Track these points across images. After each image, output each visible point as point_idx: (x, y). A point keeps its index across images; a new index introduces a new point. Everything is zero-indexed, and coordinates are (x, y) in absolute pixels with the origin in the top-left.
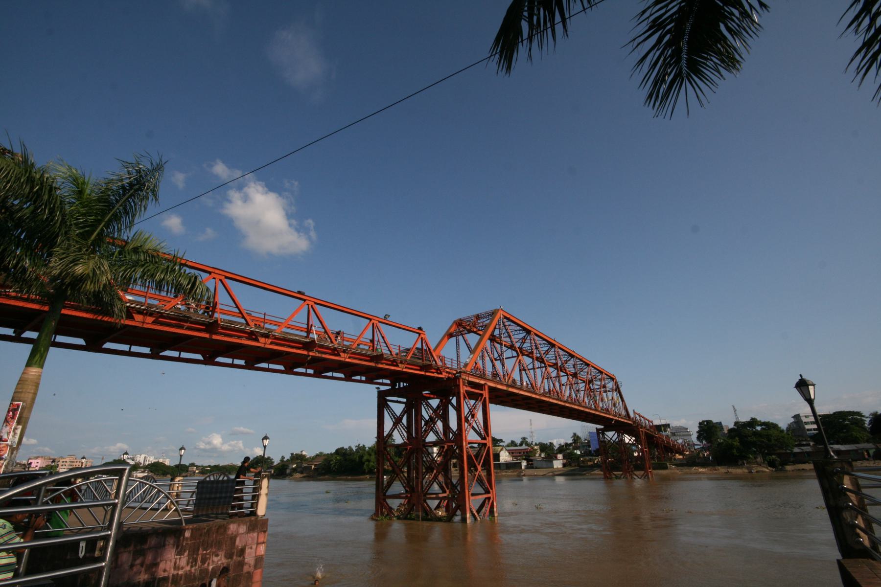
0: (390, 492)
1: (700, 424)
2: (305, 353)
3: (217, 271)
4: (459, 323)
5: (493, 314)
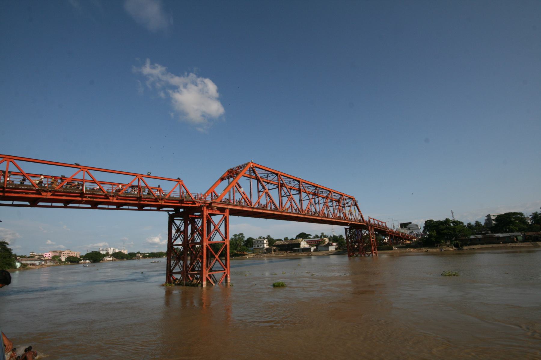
0: (174, 271)
1: (426, 222)
3: (7, 157)
5: (247, 164)
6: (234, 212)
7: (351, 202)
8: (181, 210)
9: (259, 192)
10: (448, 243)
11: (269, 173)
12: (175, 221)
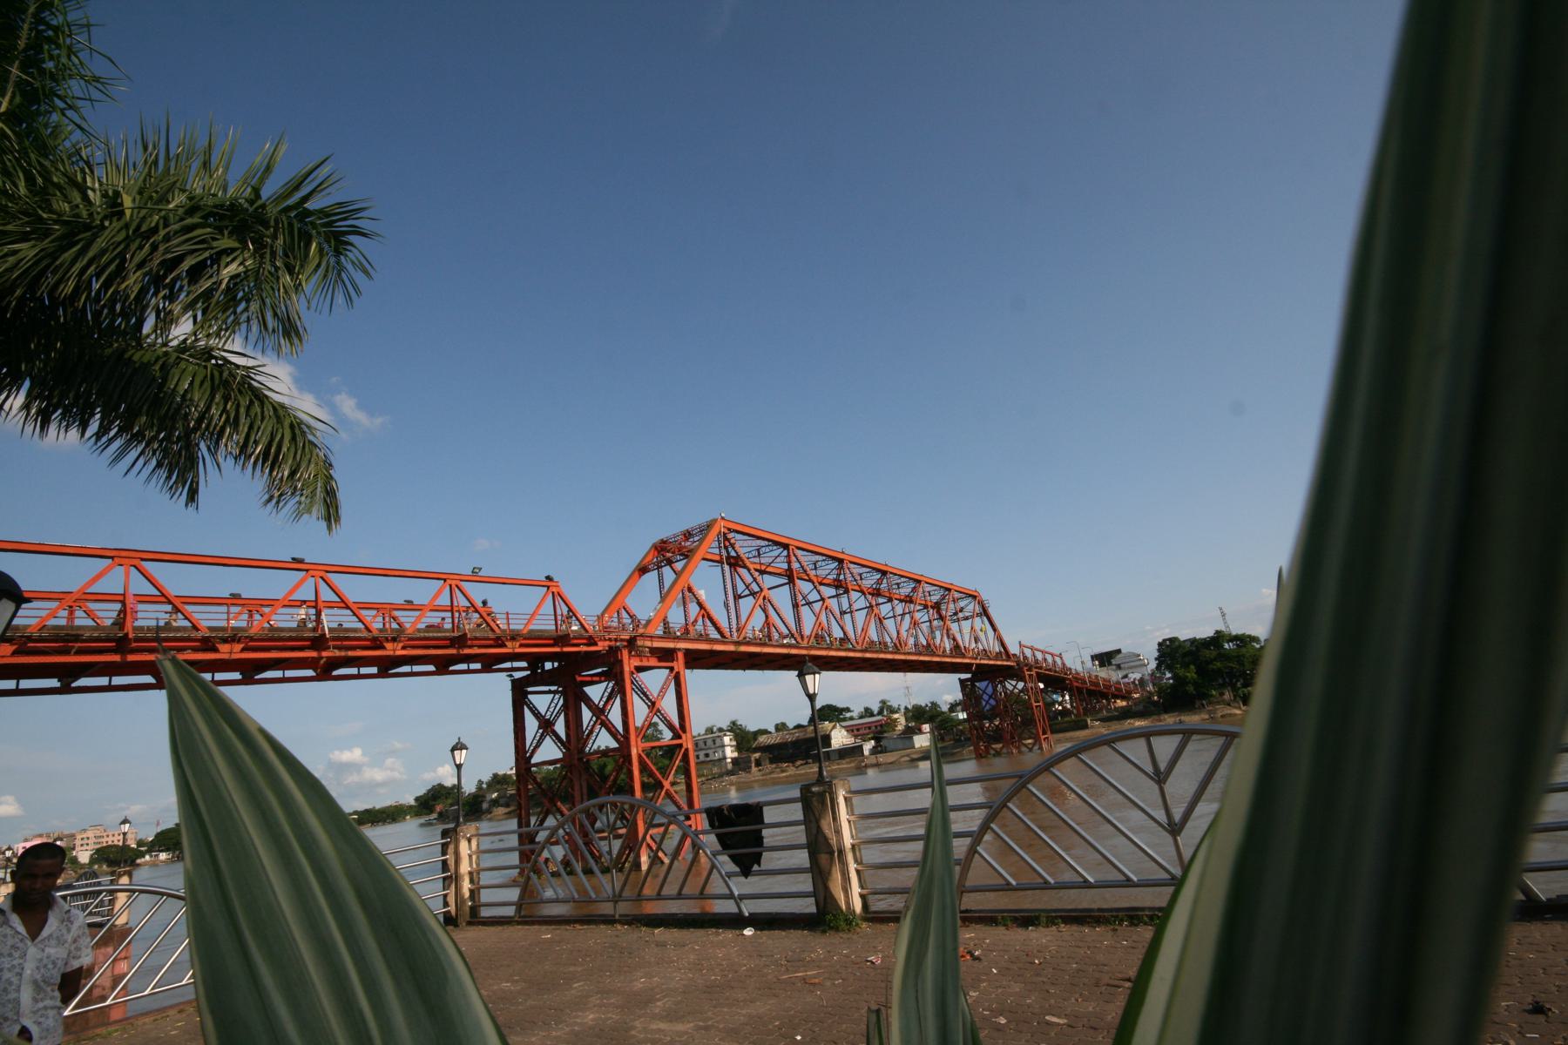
1: (1160, 644)
2: (314, 654)
4: (661, 548)
5: (709, 526)
6: (698, 660)
7: (971, 607)
8: (548, 666)
9: (737, 597)
10: (1227, 696)
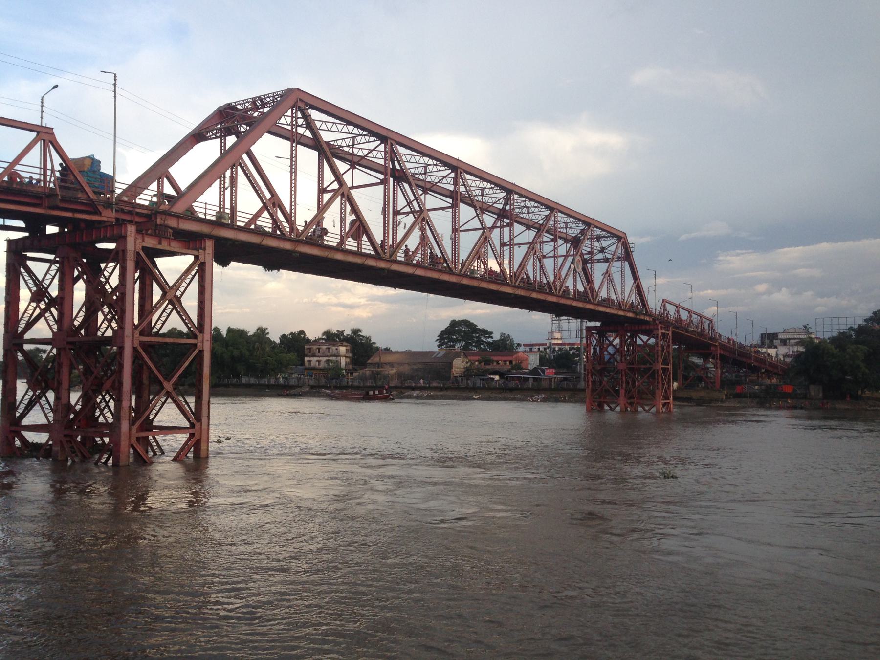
0: (25, 422)
7: (613, 248)
8: (51, 230)
9: (322, 191)
11: (356, 131)
12: (30, 263)
